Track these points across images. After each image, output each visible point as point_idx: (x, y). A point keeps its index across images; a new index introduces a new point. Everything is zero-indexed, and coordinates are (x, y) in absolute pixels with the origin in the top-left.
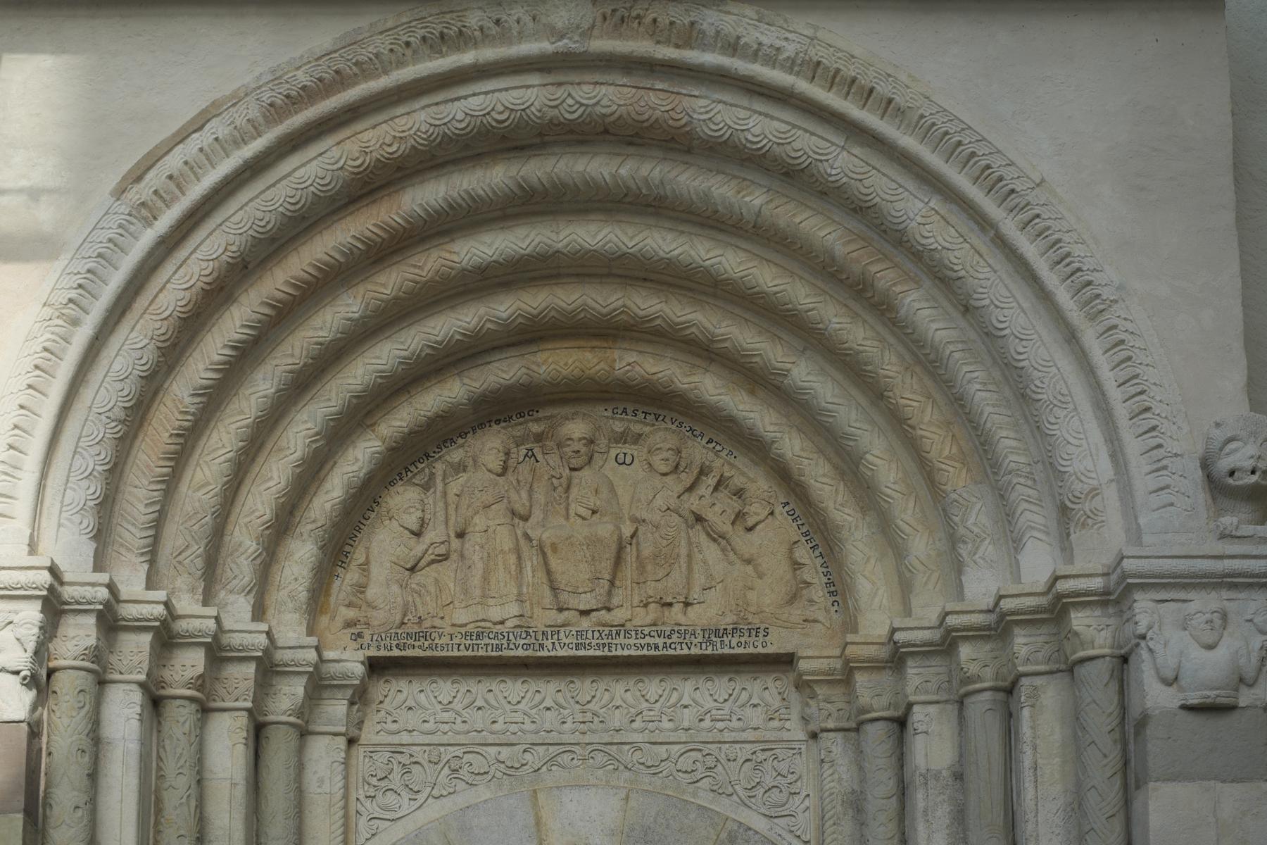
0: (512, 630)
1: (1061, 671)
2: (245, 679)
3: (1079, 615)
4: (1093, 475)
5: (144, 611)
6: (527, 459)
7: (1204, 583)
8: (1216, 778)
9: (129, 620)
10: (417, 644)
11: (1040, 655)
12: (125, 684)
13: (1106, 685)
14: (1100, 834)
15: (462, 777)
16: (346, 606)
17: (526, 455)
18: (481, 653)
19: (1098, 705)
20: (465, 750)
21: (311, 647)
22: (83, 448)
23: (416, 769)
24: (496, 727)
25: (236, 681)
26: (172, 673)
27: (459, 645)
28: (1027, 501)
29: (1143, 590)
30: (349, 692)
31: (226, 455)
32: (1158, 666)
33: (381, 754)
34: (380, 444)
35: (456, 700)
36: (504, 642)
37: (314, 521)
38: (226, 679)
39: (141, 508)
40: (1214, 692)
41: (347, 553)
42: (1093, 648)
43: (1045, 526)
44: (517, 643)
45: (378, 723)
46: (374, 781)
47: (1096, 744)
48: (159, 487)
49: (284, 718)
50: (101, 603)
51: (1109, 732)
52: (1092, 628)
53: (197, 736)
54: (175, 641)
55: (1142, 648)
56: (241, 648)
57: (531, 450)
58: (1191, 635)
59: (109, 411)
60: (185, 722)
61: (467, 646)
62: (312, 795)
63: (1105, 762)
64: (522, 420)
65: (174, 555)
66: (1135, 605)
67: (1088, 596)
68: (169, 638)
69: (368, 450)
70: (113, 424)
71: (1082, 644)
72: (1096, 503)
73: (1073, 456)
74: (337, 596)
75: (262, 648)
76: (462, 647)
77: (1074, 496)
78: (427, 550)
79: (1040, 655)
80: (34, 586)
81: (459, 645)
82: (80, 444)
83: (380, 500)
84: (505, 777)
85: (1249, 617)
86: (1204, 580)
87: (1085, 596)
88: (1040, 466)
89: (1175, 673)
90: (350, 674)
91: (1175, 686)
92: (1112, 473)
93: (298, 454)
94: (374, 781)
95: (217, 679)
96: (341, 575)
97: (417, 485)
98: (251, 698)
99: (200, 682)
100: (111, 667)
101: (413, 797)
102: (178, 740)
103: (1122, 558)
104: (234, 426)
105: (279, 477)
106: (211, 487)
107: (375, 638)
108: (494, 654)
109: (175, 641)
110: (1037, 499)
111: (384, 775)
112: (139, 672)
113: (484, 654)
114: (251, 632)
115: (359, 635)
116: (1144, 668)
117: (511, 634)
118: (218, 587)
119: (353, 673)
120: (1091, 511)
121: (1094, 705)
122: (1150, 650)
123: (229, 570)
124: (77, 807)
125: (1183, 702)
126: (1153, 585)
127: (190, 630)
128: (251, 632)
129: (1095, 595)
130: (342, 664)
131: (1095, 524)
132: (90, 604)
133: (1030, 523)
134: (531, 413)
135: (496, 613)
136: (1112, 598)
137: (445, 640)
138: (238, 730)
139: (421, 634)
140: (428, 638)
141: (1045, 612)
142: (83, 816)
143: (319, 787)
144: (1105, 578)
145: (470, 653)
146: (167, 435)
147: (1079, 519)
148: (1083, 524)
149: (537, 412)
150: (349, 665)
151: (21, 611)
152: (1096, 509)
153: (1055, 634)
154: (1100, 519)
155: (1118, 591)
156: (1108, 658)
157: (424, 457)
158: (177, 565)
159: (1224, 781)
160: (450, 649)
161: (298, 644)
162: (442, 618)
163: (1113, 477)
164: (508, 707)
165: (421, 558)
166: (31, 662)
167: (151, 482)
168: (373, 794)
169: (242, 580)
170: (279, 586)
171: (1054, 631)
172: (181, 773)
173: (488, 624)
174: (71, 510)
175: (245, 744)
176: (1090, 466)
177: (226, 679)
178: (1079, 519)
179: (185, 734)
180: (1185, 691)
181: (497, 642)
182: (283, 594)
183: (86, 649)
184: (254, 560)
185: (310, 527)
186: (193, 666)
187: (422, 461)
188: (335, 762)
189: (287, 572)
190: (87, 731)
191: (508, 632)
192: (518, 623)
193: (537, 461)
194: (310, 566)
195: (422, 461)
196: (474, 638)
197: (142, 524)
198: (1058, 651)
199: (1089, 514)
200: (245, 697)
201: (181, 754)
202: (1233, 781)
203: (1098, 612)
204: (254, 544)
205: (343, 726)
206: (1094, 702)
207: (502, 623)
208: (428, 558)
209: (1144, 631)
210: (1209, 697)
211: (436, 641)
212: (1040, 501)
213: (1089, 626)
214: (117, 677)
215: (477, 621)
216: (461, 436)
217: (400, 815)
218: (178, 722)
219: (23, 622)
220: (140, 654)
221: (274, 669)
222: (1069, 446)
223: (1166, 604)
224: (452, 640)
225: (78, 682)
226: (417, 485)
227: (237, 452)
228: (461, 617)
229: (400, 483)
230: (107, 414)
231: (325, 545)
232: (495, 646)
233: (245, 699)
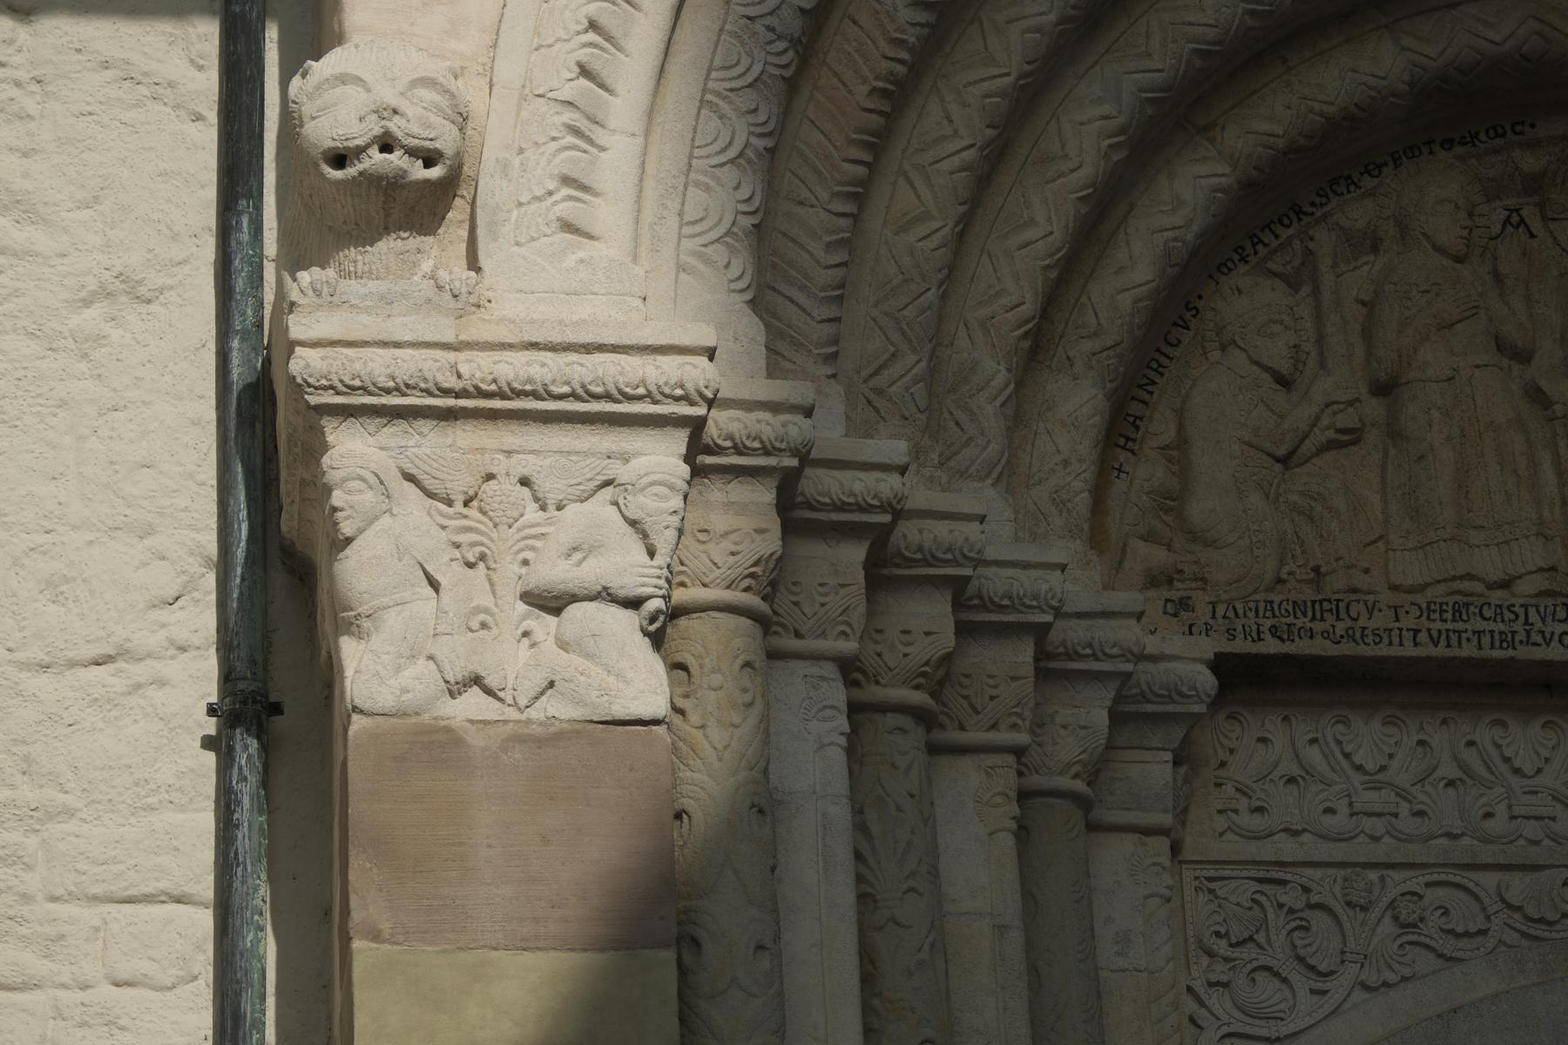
0: (1533, 601)
5: (858, 487)
6: (1510, 229)
9: (820, 507)
10: (1318, 627)
12: (807, 663)
15: (1427, 941)
16: (1141, 538)
17: (1507, 221)
18: (1468, 651)
20: (1428, 878)
22: (718, 94)
23: (1318, 920)
24: (1491, 826)
25: (991, 682)
27: (1416, 632)
31: (964, 155)
33: (1234, 884)
34: (1227, 170)
35: (1395, 764)
36: (1518, 626)
37: (1096, 334)
38: (967, 676)
39: (817, 249)
41: (1136, 418)
44: (1548, 630)
45: (1220, 812)
46: (1221, 947)
49: (1065, 782)
54: (885, 572)
56: (1005, 602)
57: (1517, 211)
59: (771, 13)
61: (1435, 634)
64: (1499, 142)
65: (864, 374)
69: (1204, 182)
70: (781, 45)
76: (1423, 637)
78: (1318, 418)
80: (679, 392)
81: (1416, 632)
82: (711, 85)
83: (1200, 304)
84: (1525, 943)
90: (1185, 689)
93: (1086, 173)
94: (1221, 947)
96: (1126, 468)
97: (1275, 274)
98: (1027, 723)
101: (1320, 986)
102: (899, 809)
104: (978, 90)
105: (1049, 220)
106: (935, 225)
107: (1220, 610)
108: (1497, 654)
109: (885, 572)
111: (1246, 935)
112: (843, 633)
113: (1475, 653)
114: (1026, 566)
115: (1184, 604)
117: (1532, 611)
123: (952, 424)
128: (1026, 566)
130: (1163, 666)
134: (1518, 128)
135: (1489, 563)
137: (1382, 620)
138: (998, 799)
139: (1326, 605)
140: (1343, 615)
143: (1118, 954)
145: (1440, 651)
146: (864, 89)
149: (1532, 126)
151: (638, 454)
157: (1292, 215)
158: (872, 397)
160: (1396, 640)
161: (1099, 608)
162: (1367, 571)
164: (1515, 781)
165: (1306, 436)
168: (1224, 978)
169: (985, 449)
172: (911, 890)
173: (1479, 587)
174: (700, 234)
177: (967, 676)
179: (912, 796)
181: (1502, 627)
183: (756, 564)
184: (1002, 405)
185: (1088, 346)
186: (927, 634)
187: (1286, 221)
188: (1152, 896)
191: (1525, 607)
192: (1545, 585)
193: (1532, 236)
195: (1286, 221)
196: (1449, 616)
197: (823, 289)
200: (1014, 719)
204: (1002, 368)
205: (1166, 811)
207: (1505, 584)
208: (1320, 436)
211: (1362, 622)
215: (1454, 578)
216: (1368, 172)
217: (1292, 1028)
218: (894, 766)
219: (644, 481)
220: (843, 591)
224: (1397, 620)
226: (1275, 274)
227: (982, 149)
228: (1410, 570)
229: (1243, 268)
230: (768, 21)
232: (1497, 637)
233: (1014, 726)
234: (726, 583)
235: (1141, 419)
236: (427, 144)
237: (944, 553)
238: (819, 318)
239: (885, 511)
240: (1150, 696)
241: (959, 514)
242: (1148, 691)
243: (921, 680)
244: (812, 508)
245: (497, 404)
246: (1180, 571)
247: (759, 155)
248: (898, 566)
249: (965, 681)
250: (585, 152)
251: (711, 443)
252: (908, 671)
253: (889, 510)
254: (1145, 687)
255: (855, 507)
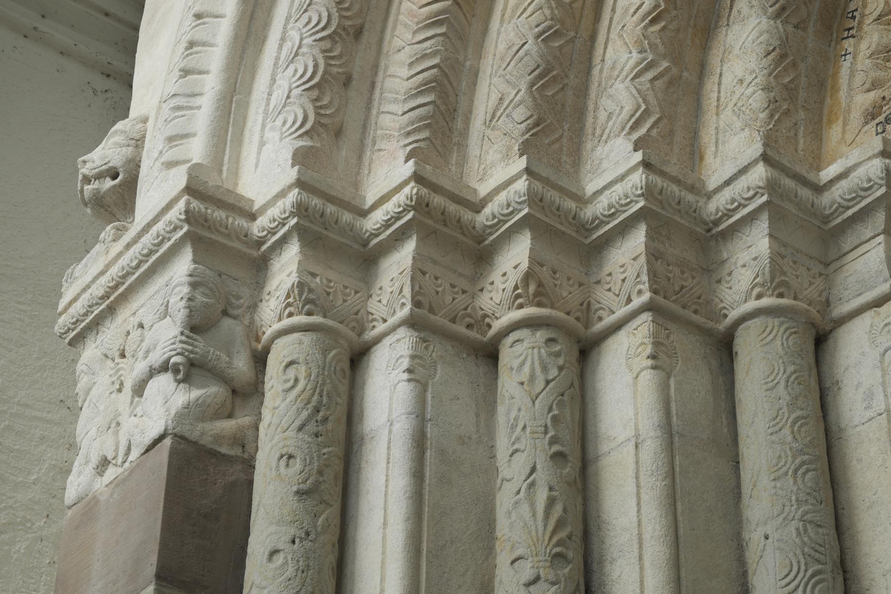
2: (635, 259)
21: (754, 162)
25: (622, 270)
26: (490, 295)
30: (880, 219)
48: (430, 33)
49: (752, 305)
50: (292, 214)
53: (548, 382)
56: (613, 210)
60: (523, 364)
62: (858, 429)
68: (480, 243)
74: (849, 85)
75: (639, 192)
90: (866, 185)
95: (598, 282)
96: (850, 50)
99: (532, 288)
100: (371, 317)
109: (487, 242)
118: (589, 145)
119: (870, 180)
124: (274, 552)
127: (496, 211)
130: (853, 175)
132: (284, 225)
142: (286, 563)
150: (861, 172)
166: (181, 342)
167: (415, 33)
169: (619, 114)
170: (718, 107)
172: (517, 451)
175: (654, 368)
179: (522, 383)
182: (727, 115)
183: (288, 296)
189: (727, 79)
190: (297, 423)
194: (761, 50)
201: (516, 419)
214: (381, 328)
218: (512, 369)
221: (714, 232)
225: (285, 352)
231: (783, 9)
233: (640, 292)
234: (277, 319)
235: (856, 10)
236: (104, 167)
237: (507, 209)
238: (400, 113)
239: (409, 211)
240: (845, 204)
241: (512, 177)
242: (842, 201)
243: (520, 301)
244: (377, 236)
245: (121, 289)
246: (884, 98)
247: (311, 46)
248: (491, 234)
249: (609, 279)
250: (183, 116)
251: (257, 238)
252: (507, 300)
253: (409, 208)
254: (839, 200)
255: (393, 220)
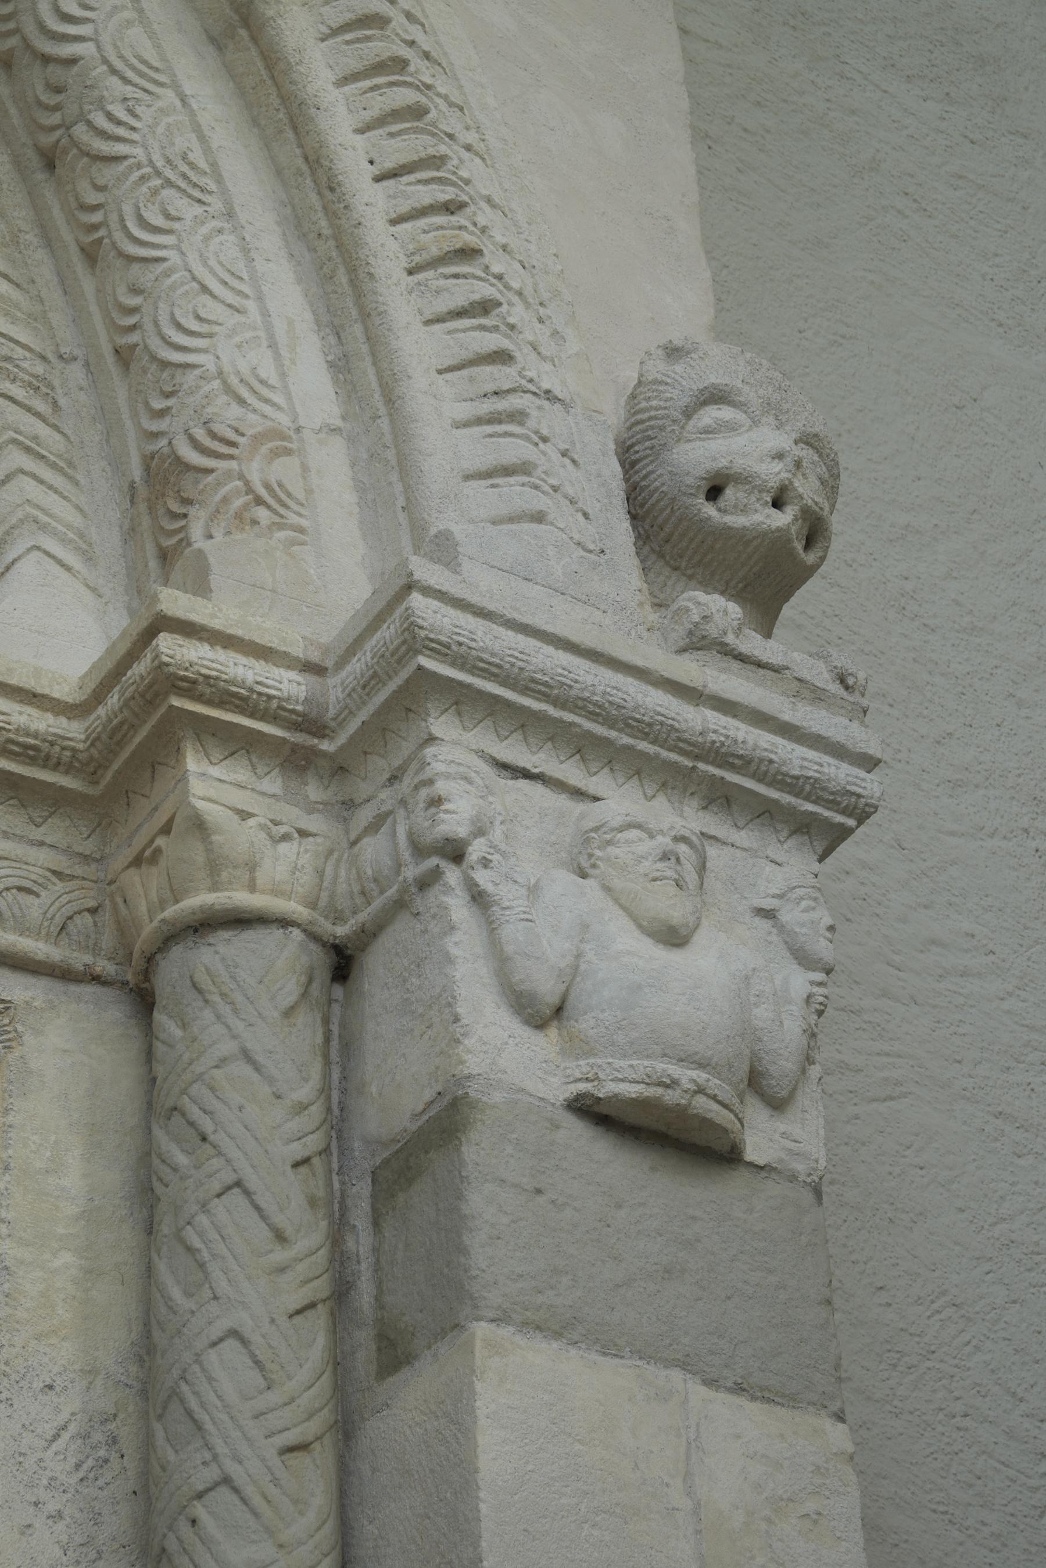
1: (96, 979)
3: (215, 771)
4: (278, 398)
7: (642, 754)
8: (684, 1365)
11: (34, 908)
13: (289, 1013)
14: (257, 1501)
19: (257, 1068)
28: (28, 450)
29: (459, 714)
32: (509, 949)
40: (694, 1074)
42: (252, 888)
43: (81, 536)
47: (247, 1193)
51: (296, 1165)
52: (252, 822)
55: (449, 890)
58: (607, 889)
63: (280, 1255)
66: (430, 751)
67: (253, 714)
71: (214, 866)
72: (285, 470)
73: (216, 329)
77: (213, 435)
79: (34, 908)
85: (768, 903)
86: (643, 746)
87: (242, 711)
88: (76, 373)
89: (563, 987)
91: (553, 1032)
92: (336, 411)
103: (409, 587)
110: (59, 456)
116: (454, 951)
120: (267, 486)
121: (248, 1071)
122: (478, 898)
125: (583, 1087)
126: (494, 706)
129: (274, 718)
131: (281, 527)
133: (29, 509)
136: (325, 746)
141: (69, 770)
144: (312, 679)
147: (225, 500)
148: (238, 516)
152: (280, 485)
153: (85, 858)
154: (294, 519)
155: (353, 726)
156: (296, 933)
159: (710, 1383)
163: (339, 423)
171: (88, 847)
176: (268, 371)
178: (225, 500)
180: (591, 1053)
198: (93, 911)
199: (263, 492)
202: (739, 1389)
203: (273, 784)
206: (247, 1056)
209: (462, 832)
210: (674, 1084)
212: (70, 464)
213: (244, 815)
222: (205, 298)
223: (522, 783)
